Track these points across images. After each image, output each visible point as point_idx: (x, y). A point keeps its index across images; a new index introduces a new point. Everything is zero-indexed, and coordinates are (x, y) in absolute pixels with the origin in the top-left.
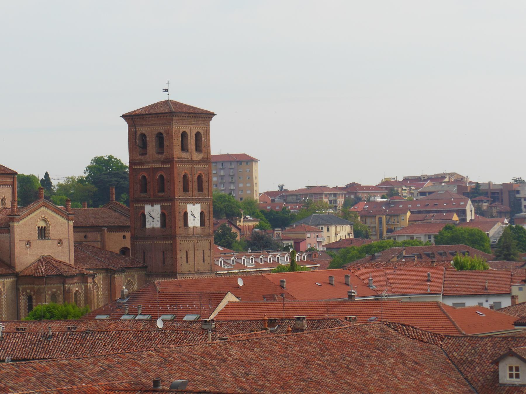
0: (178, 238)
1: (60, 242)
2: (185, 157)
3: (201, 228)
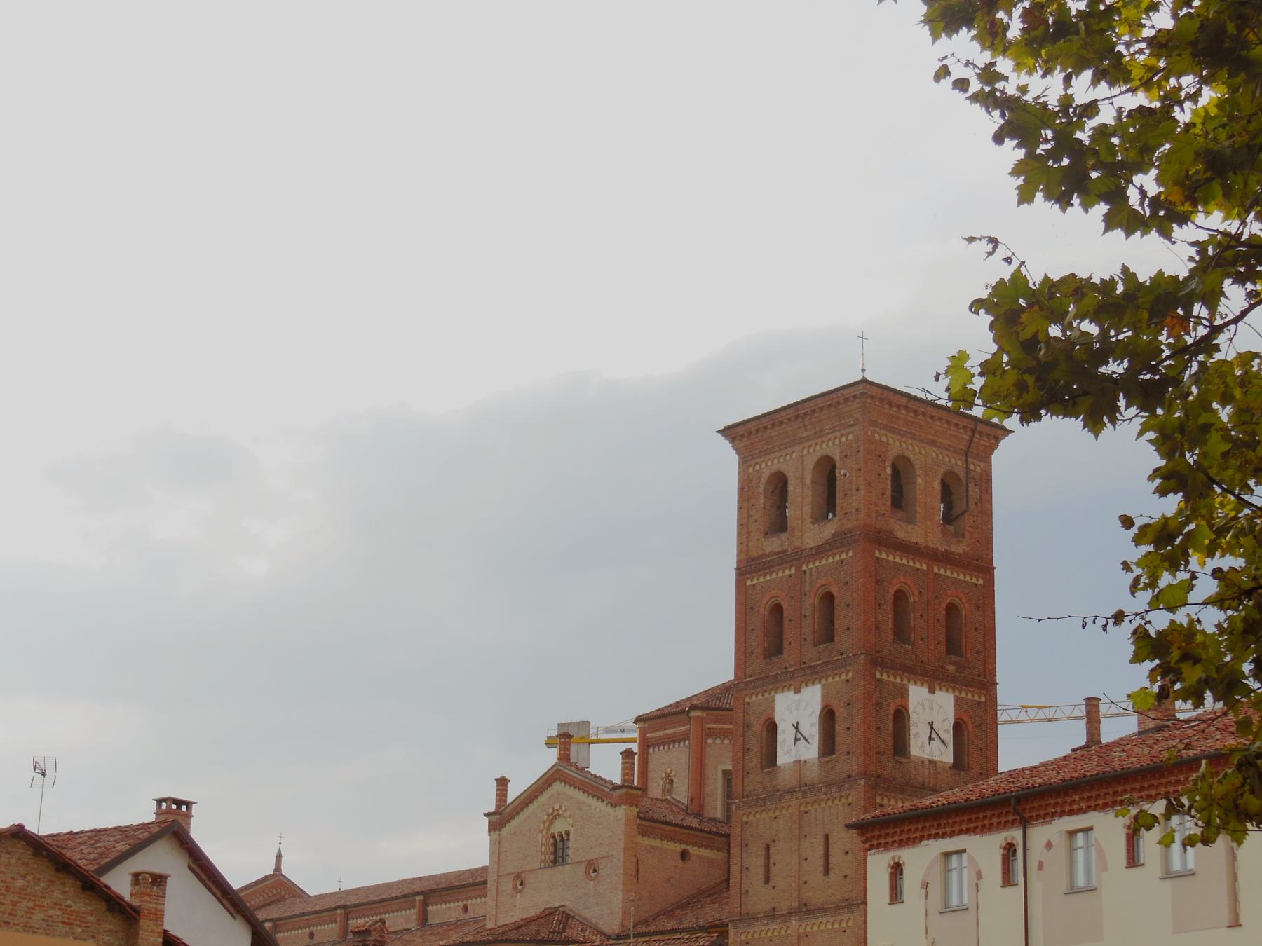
0: (738, 808)
1: (592, 867)
2: (776, 550)
3: (820, 762)
